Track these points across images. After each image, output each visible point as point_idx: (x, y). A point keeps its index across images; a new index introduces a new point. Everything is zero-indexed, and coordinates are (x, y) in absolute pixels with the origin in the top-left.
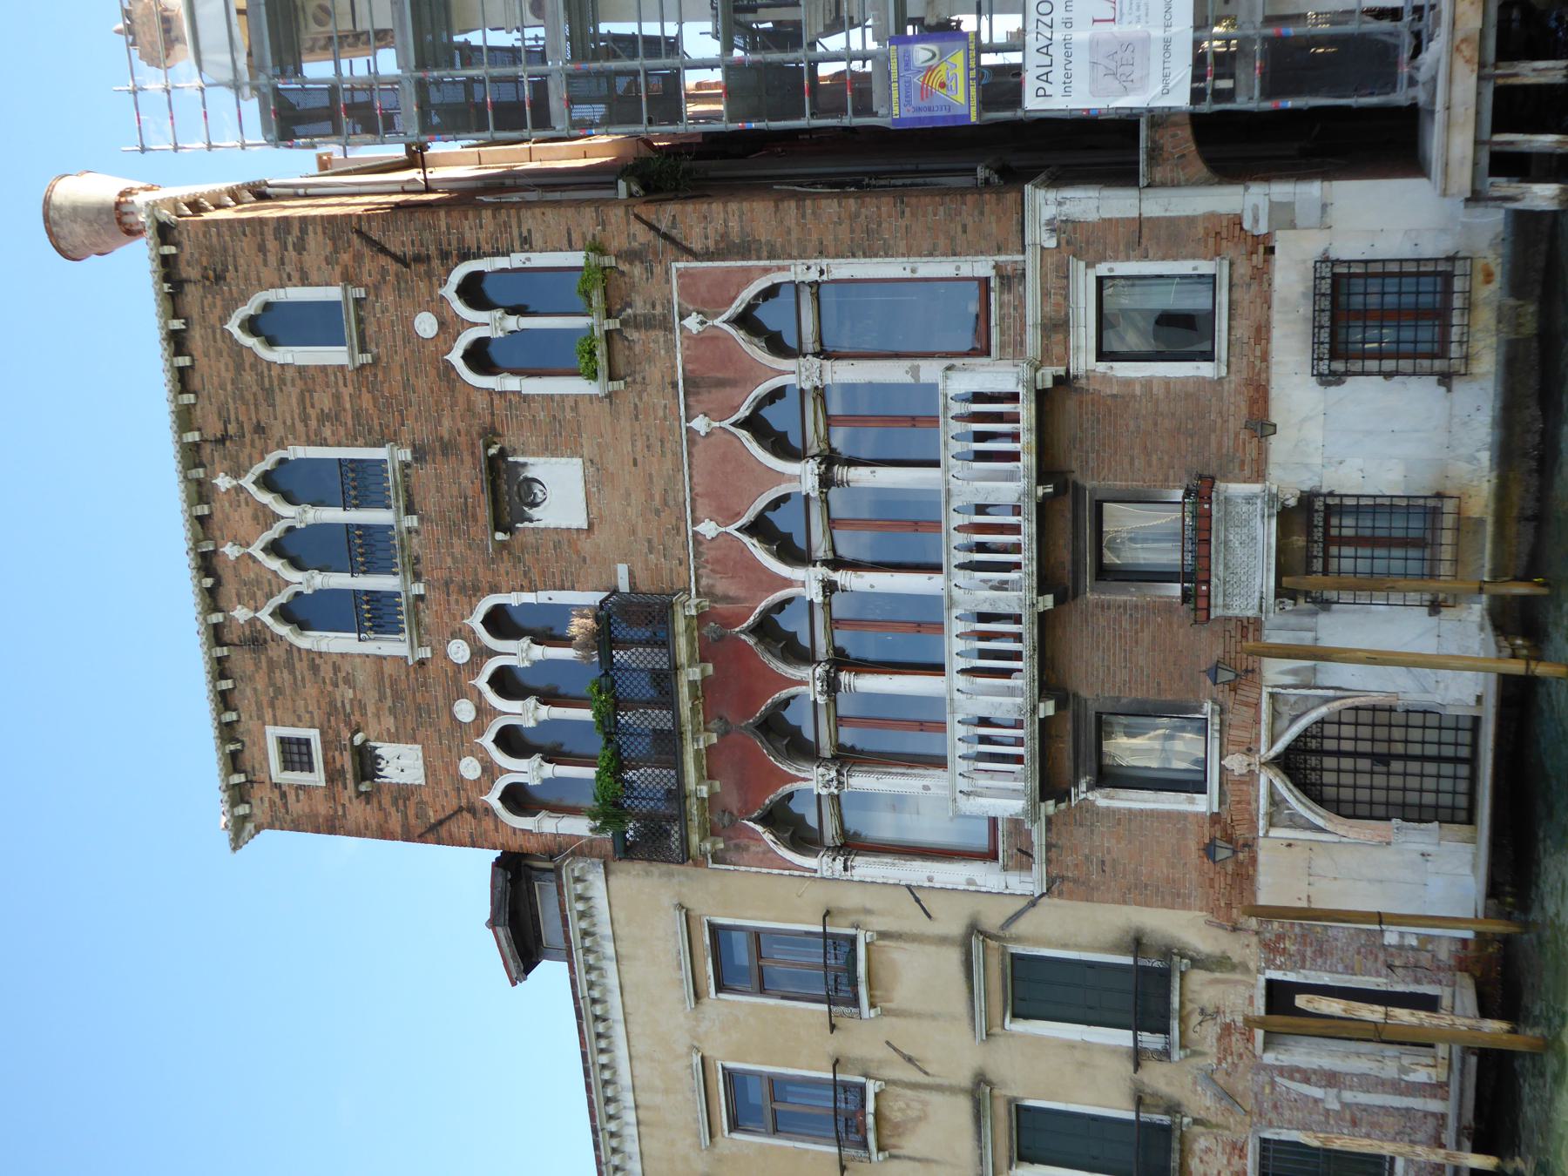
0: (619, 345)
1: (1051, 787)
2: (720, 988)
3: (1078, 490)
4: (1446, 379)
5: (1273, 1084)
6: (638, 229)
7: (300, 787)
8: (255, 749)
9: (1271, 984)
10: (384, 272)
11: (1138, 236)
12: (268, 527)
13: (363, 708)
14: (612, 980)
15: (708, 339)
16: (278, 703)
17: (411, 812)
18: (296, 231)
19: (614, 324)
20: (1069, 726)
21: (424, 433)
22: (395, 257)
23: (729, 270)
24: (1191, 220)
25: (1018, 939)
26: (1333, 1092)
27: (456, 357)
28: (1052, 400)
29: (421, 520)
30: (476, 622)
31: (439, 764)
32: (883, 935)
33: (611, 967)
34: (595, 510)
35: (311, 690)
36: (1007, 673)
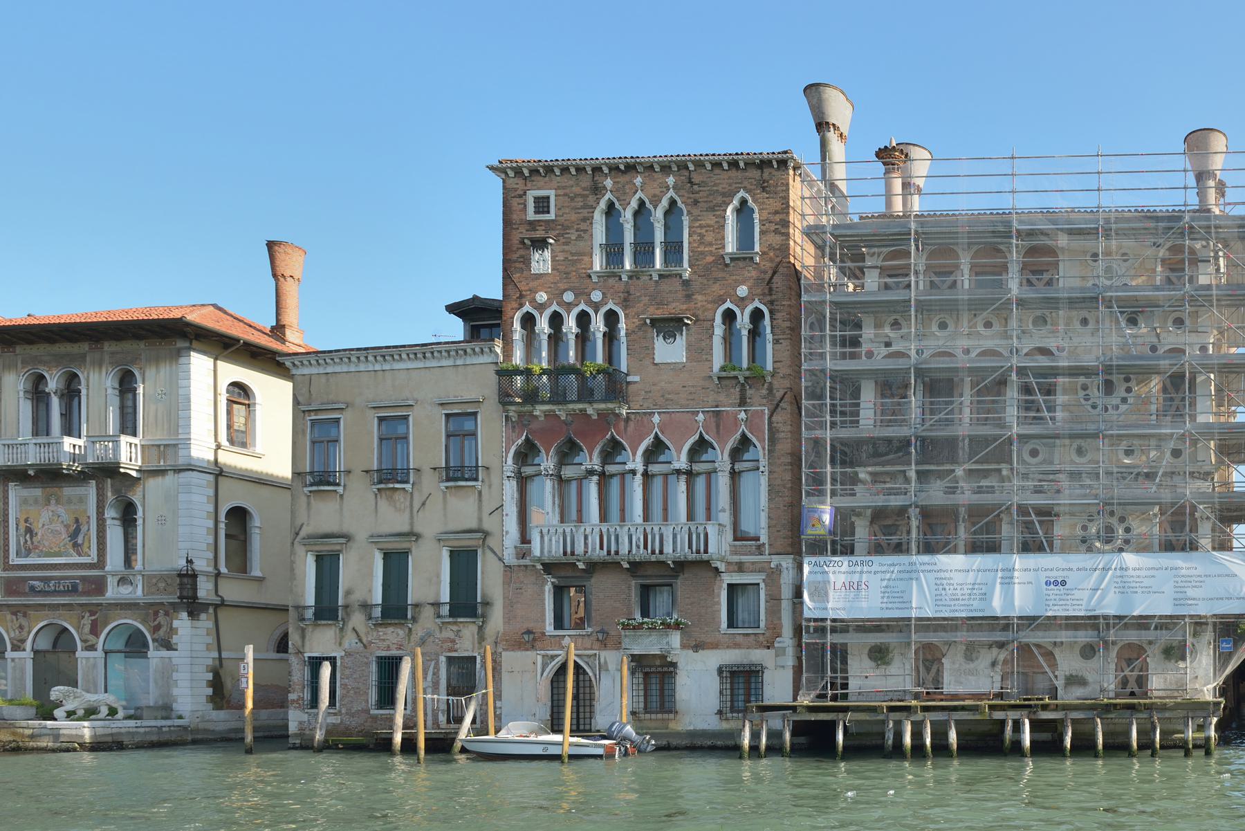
0: (734, 382)
2: (447, 416)
3: (676, 577)
4: (720, 712)
6: (782, 392)
8: (542, 183)
9: (475, 658)
10: (765, 272)
13: (567, 244)
14: (444, 363)
15: (736, 422)
19: (742, 380)
21: (696, 286)
22: (771, 278)
24: (780, 619)
27: (728, 305)
30: (610, 305)
32: (480, 493)
33: (450, 362)
35: (574, 217)
36: (601, 548)
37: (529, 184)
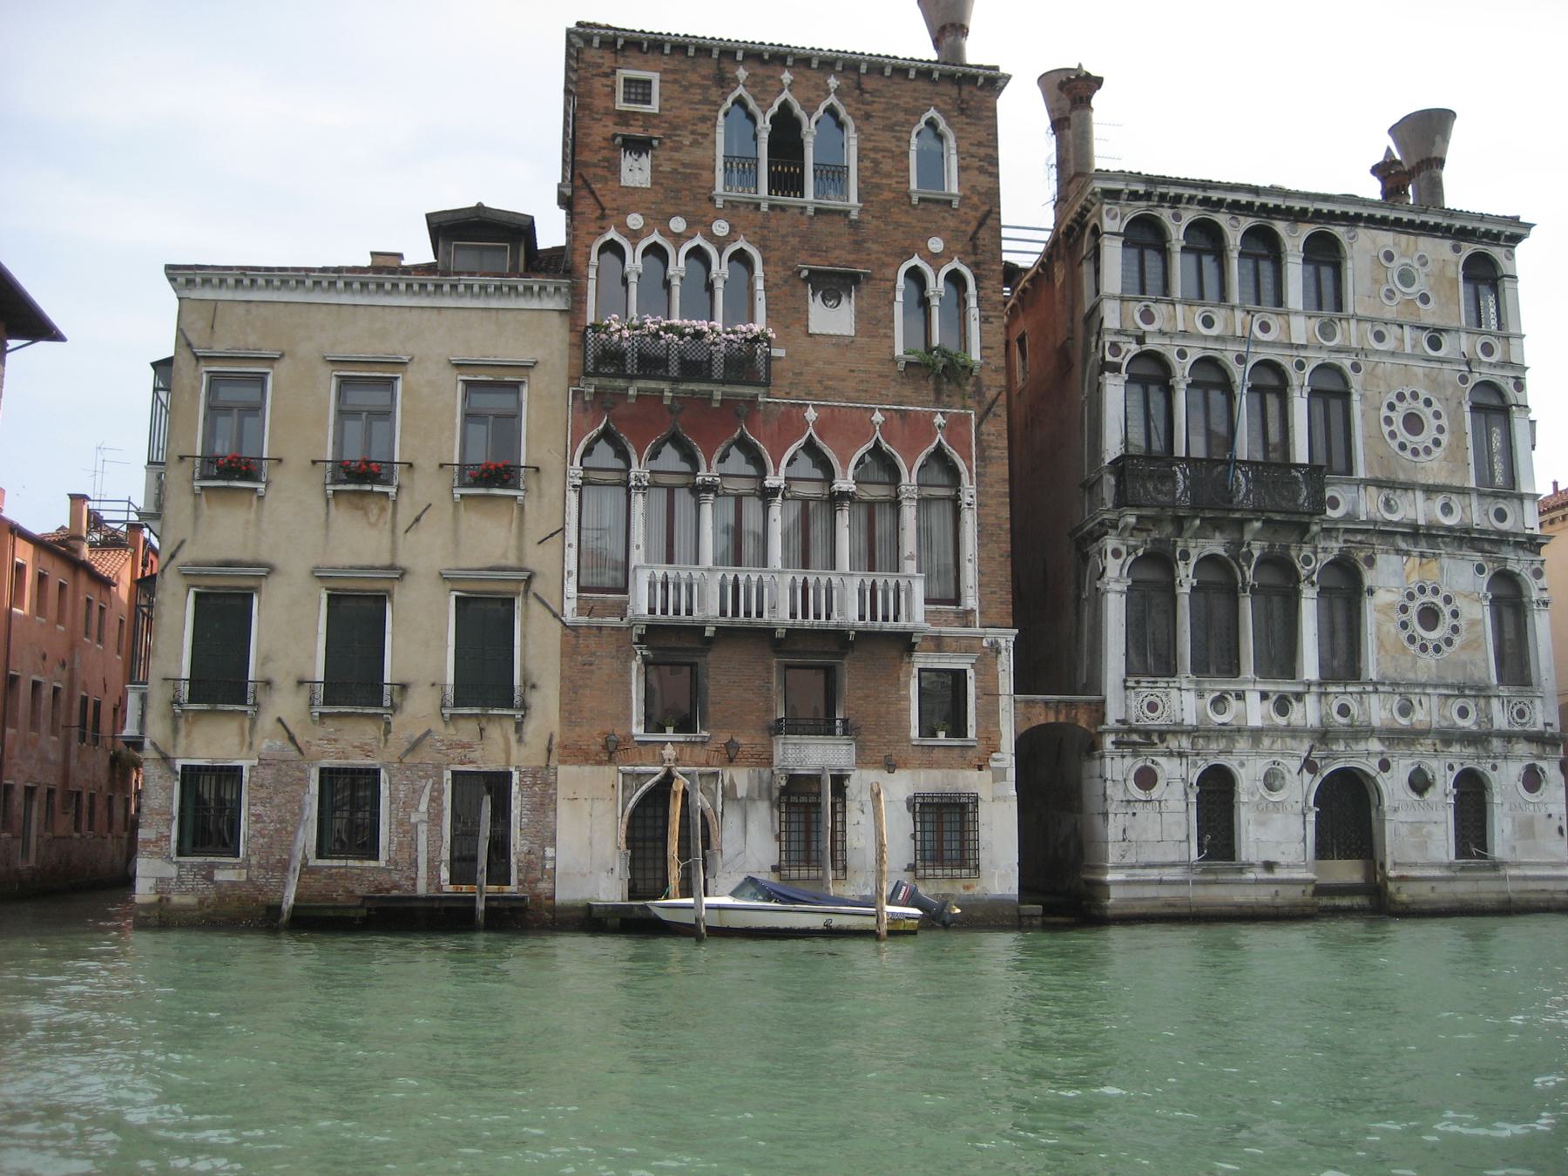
1: (653, 633)
3: (842, 656)
4: (912, 868)
5: (427, 777)
7: (614, 91)
10: (968, 223)
11: (989, 694)
12: (803, 108)
15: (930, 431)
16: (676, 87)
17: (599, 171)
18: (991, 169)
20: (687, 645)
22: (976, 233)
23: (970, 446)
25: (526, 604)
26: (425, 817)
27: (916, 261)
28: (904, 643)
29: (811, 218)
30: (741, 244)
31: (637, 198)
32: (522, 508)
34: (820, 339)
37: (621, 61)
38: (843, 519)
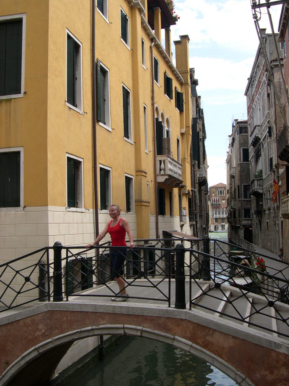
1: (215, 218)
38: (224, 212)
